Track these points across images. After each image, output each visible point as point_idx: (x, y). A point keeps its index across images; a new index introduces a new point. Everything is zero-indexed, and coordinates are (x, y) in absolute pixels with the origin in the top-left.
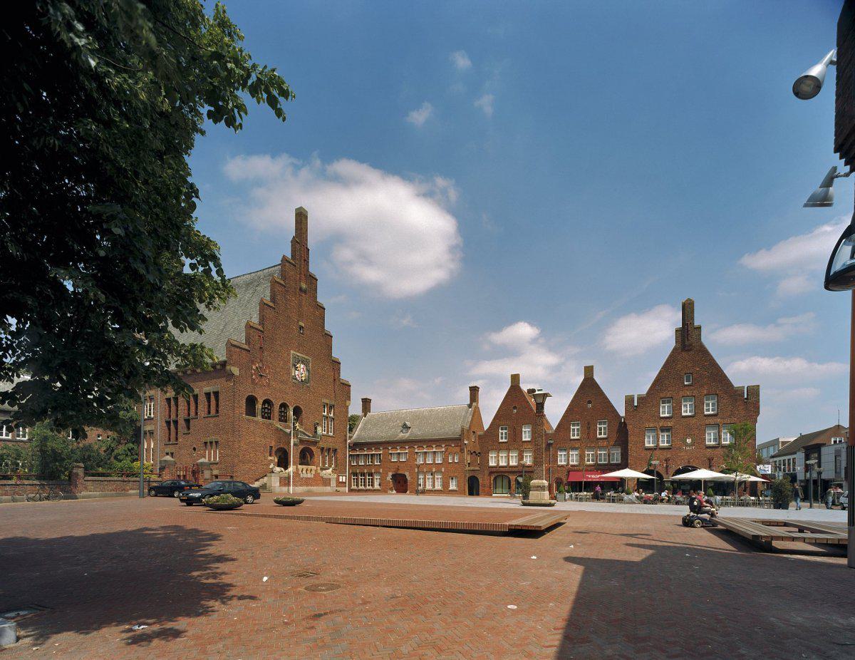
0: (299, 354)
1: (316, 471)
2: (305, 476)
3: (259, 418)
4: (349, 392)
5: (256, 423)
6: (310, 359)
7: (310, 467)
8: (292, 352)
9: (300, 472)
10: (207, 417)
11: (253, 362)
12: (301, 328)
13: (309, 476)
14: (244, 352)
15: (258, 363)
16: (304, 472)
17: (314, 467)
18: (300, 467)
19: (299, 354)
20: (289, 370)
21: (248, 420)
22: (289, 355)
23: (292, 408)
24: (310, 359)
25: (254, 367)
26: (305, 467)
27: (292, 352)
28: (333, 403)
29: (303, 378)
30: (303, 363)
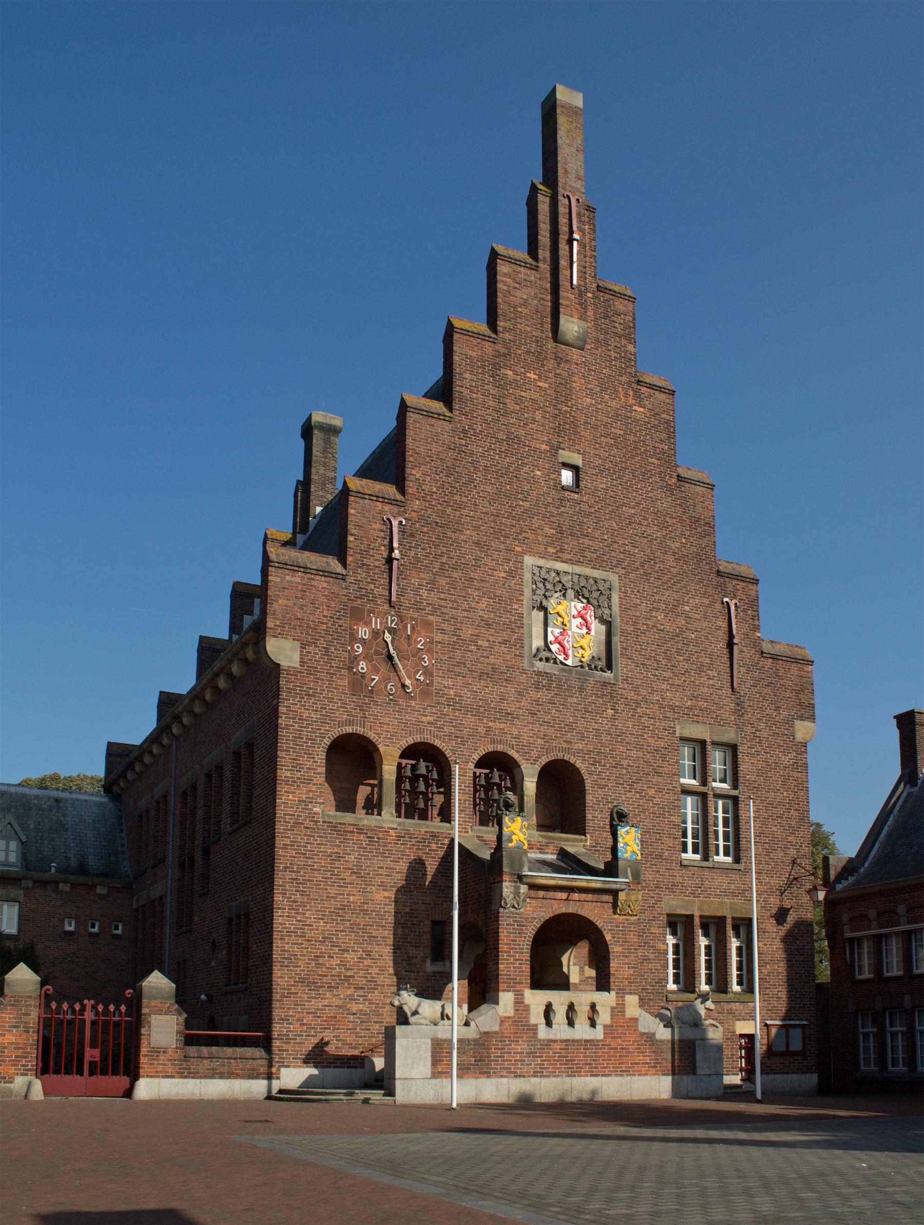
0: (560, 566)
1: (618, 1010)
2: (560, 1030)
3: (388, 817)
4: (805, 688)
5: (373, 836)
6: (614, 578)
8: (529, 561)
9: (537, 1017)
10: (235, 831)
11: (358, 615)
13: (582, 1031)
14: (321, 583)
15: (383, 615)
16: (560, 1016)
17: (606, 1000)
18: (536, 999)
19: (560, 566)
20: (518, 625)
22: (514, 573)
23: (537, 768)
24: (614, 578)
25: (363, 632)
26: (559, 999)
27: (529, 561)
28: (729, 736)
30: (578, 595)
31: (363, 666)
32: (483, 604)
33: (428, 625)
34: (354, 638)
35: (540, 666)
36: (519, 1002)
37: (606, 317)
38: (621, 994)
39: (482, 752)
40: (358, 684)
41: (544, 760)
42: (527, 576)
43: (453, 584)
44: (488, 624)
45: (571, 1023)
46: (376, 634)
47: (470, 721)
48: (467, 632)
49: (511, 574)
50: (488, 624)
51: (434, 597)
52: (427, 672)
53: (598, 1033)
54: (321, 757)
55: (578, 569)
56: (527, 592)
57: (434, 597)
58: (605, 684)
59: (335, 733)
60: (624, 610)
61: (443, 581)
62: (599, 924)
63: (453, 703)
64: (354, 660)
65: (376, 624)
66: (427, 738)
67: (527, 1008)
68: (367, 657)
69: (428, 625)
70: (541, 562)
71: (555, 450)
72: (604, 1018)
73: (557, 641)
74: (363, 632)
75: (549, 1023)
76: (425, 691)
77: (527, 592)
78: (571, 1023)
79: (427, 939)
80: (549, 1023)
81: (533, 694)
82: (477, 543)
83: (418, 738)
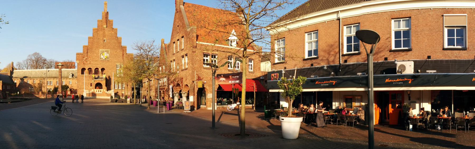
0: (103, 50)
1: (103, 91)
6: (109, 50)
7: (100, 90)
9: (95, 91)
11: (84, 57)
12: (104, 40)
13: (100, 92)
16: (98, 91)
17: (102, 90)
21: (82, 76)
23: (101, 69)
25: (84, 59)
27: (100, 50)
29: (106, 58)
30: (106, 52)
31: (84, 62)
32: (96, 55)
33: (90, 57)
34: (83, 60)
35: (101, 59)
36: (94, 90)
37: (109, 24)
38: (104, 89)
39: (95, 68)
40: (84, 64)
41: (101, 68)
42: (100, 51)
43: (93, 53)
44: (96, 56)
45: (99, 92)
46: (85, 59)
47: (94, 65)
48: (94, 58)
49: (98, 51)
50: (96, 56)
51: (91, 55)
52: (90, 61)
53: (101, 93)
54: (81, 70)
55: (105, 50)
56: (100, 53)
57: (91, 55)
58: (108, 60)
59: (82, 68)
60: (110, 53)
61: (92, 53)
62: (102, 83)
63: (92, 64)
64: (83, 62)
65: (85, 58)
66: (90, 67)
67: (95, 91)
68: (85, 61)
69: (90, 57)
70: (102, 50)
71: (103, 39)
72: (102, 91)
73: (103, 57)
74: (84, 59)
75: (97, 92)
76: (90, 63)
77: (100, 53)
78: (99, 92)
79: (90, 85)
80: (97, 92)
81: (100, 62)
82: (95, 49)
83: (89, 67)
